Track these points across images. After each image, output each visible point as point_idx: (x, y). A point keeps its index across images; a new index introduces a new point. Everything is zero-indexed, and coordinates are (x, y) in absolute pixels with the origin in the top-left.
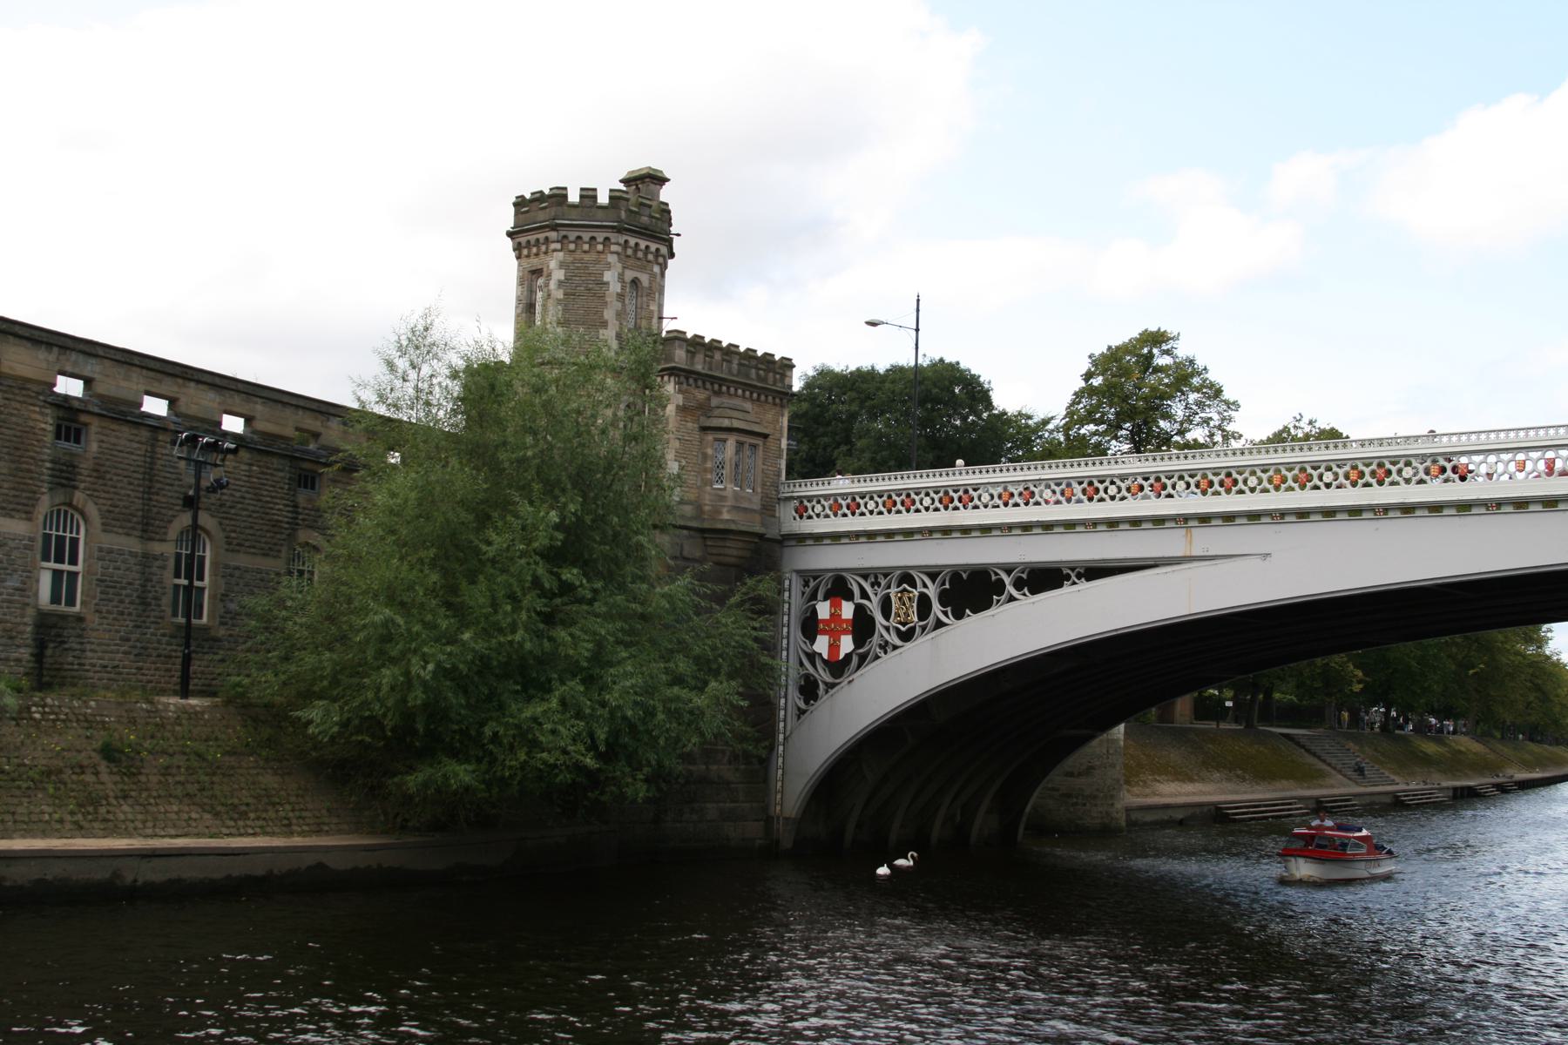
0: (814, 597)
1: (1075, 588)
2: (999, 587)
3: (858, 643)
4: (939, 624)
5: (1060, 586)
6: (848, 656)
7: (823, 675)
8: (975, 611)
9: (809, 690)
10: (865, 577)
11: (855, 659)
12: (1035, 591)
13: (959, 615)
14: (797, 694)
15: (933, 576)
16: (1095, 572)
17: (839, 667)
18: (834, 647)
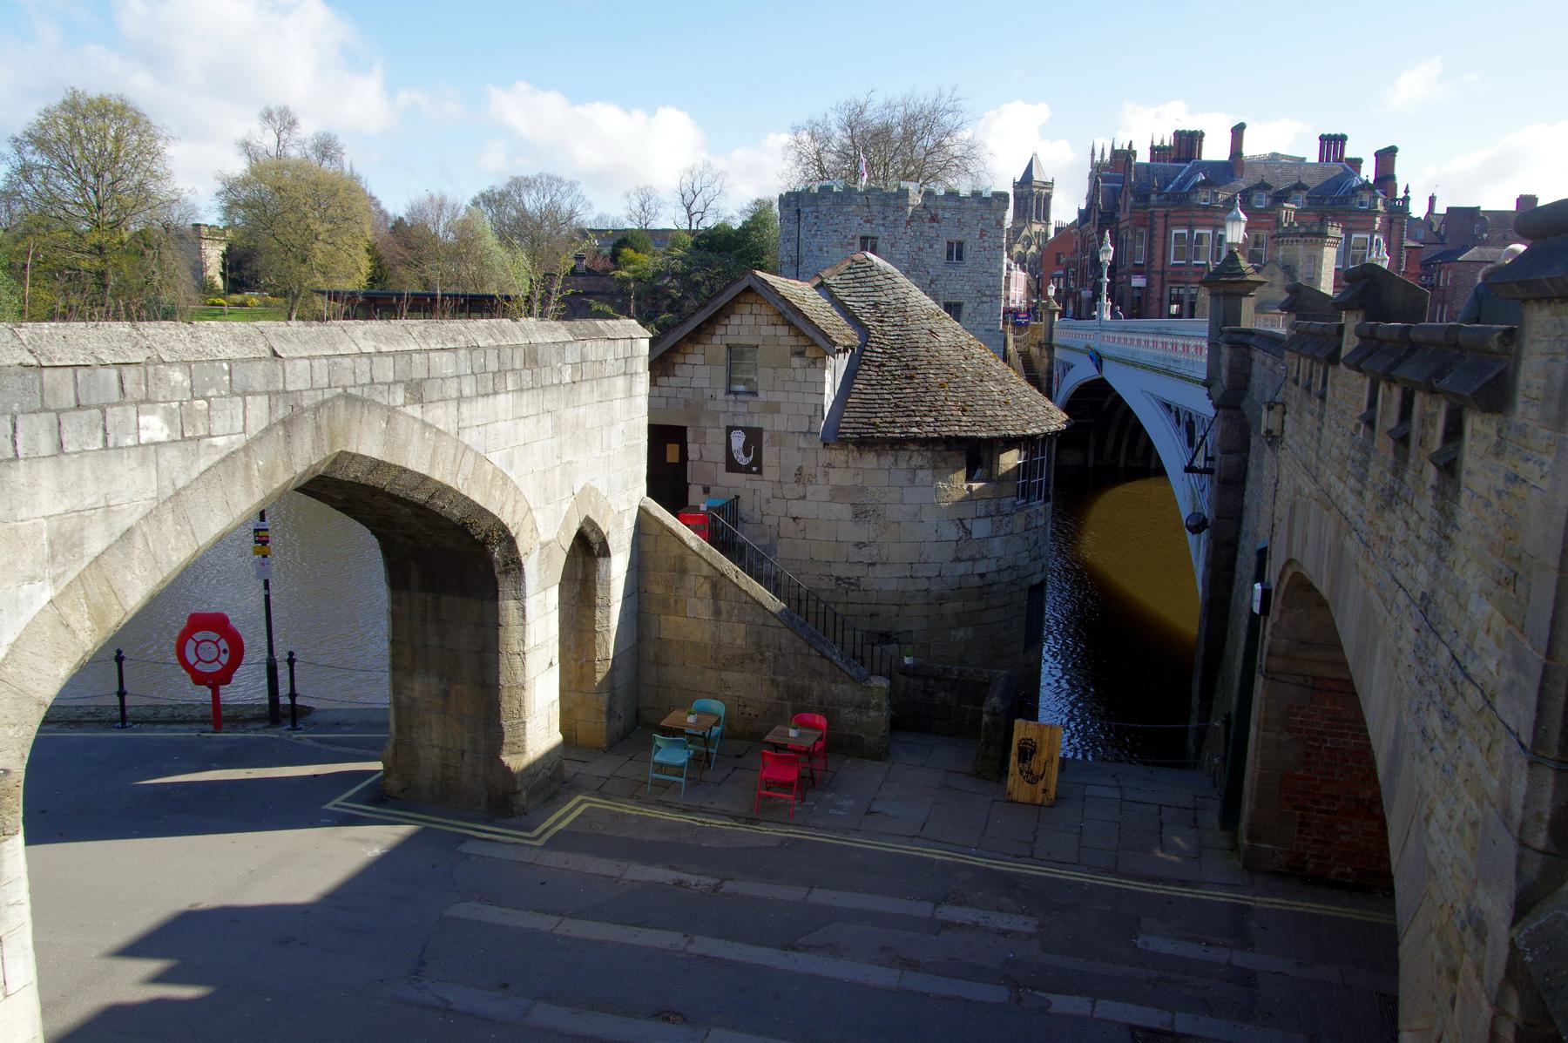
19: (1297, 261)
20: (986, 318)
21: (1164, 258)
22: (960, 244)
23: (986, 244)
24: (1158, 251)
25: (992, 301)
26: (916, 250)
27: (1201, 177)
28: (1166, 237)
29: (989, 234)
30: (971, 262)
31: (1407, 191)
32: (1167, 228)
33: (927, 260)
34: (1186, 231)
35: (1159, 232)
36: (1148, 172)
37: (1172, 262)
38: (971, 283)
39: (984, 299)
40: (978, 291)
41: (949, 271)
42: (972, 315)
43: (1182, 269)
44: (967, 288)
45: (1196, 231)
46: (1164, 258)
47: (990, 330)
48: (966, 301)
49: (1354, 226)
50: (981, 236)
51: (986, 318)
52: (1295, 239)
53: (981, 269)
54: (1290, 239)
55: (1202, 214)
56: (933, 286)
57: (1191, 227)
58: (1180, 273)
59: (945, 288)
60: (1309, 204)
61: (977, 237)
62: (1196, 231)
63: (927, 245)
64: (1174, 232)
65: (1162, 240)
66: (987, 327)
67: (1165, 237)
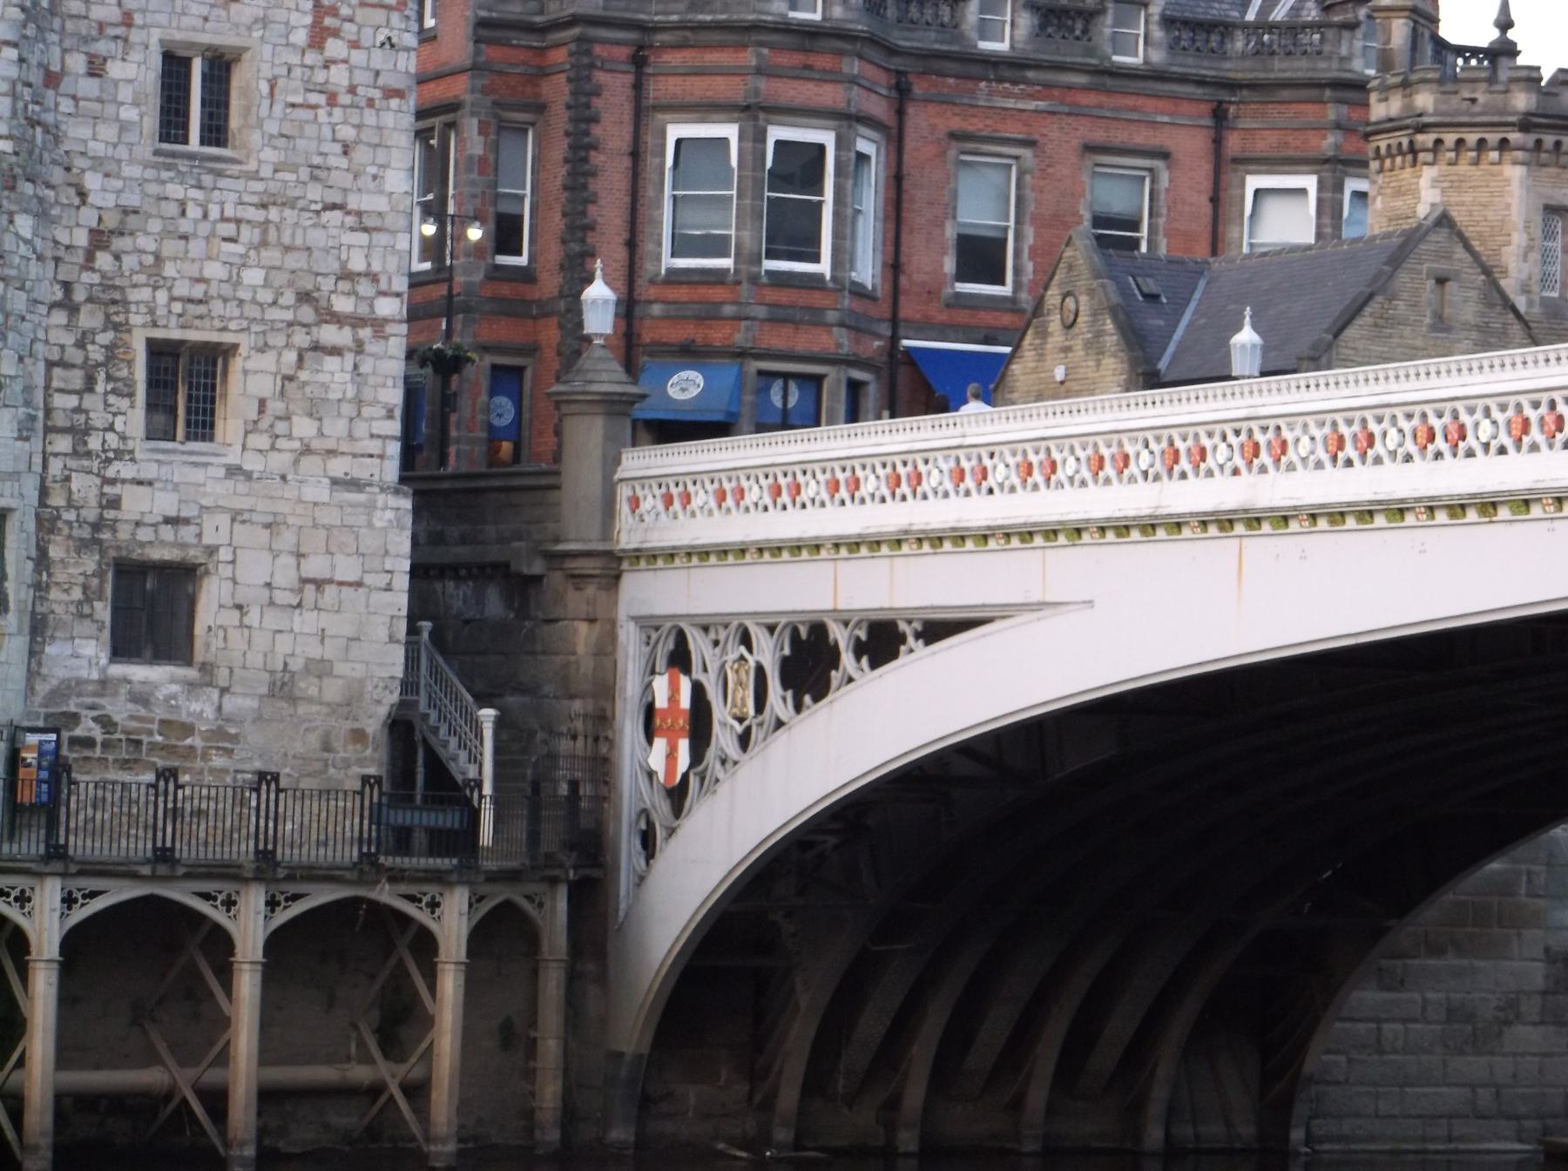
0: (653, 672)
1: (912, 656)
2: (833, 658)
3: (697, 756)
4: (780, 724)
5: (894, 655)
6: (685, 776)
7: (661, 808)
8: (816, 699)
9: (648, 842)
10: (706, 629)
11: (693, 782)
12: (875, 664)
13: (798, 707)
14: (637, 843)
15: (771, 629)
16: (936, 630)
17: (678, 795)
18: (671, 756)
20: (341, 426)
21: (632, 245)
22: (221, 66)
23: (338, 77)
25: (359, 348)
26: (36, 77)
29: (349, 29)
30: (269, 155)
31: (1505, 23)
32: (643, 113)
33: (76, 131)
34: (729, 131)
35: (613, 131)
37: (669, 262)
38: (271, 256)
39: (330, 334)
40: (304, 297)
41: (175, 190)
42: (275, 407)
43: (717, 293)
44: (253, 276)
46: (632, 245)
47: (354, 484)
48: (245, 342)
50: (319, 37)
51: (336, 427)
52: (1493, 137)
53: (315, 192)
54: (1472, 138)
55: (798, 59)
56: (104, 260)
58: (710, 314)
59: (155, 272)
60: (1173, 46)
61: (300, 37)
62: (777, 133)
63: (77, 63)
65: (627, 162)
66: (338, 467)
67: (636, 155)
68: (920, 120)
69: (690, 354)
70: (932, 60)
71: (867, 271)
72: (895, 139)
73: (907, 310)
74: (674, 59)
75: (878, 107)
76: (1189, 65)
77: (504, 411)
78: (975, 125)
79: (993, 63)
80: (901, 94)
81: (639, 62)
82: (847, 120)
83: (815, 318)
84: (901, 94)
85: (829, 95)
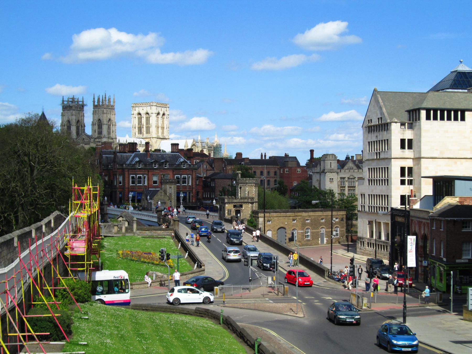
19: (167, 189)
24: (126, 182)
27: (137, 159)
28: (129, 177)
32: (129, 175)
34: (135, 176)
35: (127, 176)
36: (121, 157)
37: (131, 185)
45: (138, 176)
49: (182, 173)
57: (136, 174)
58: (133, 189)
60: (169, 166)
62: (138, 176)
64: (131, 176)
68: (150, 173)
69: (132, 191)
70: (151, 169)
71: (146, 184)
72: (148, 175)
73: (149, 187)
74: (131, 171)
75: (147, 173)
76: (171, 168)
77: (120, 195)
78: (154, 173)
79: (156, 169)
80: (148, 171)
81: (128, 171)
82: (143, 174)
83: (141, 188)
84: (148, 171)
85: (142, 173)
